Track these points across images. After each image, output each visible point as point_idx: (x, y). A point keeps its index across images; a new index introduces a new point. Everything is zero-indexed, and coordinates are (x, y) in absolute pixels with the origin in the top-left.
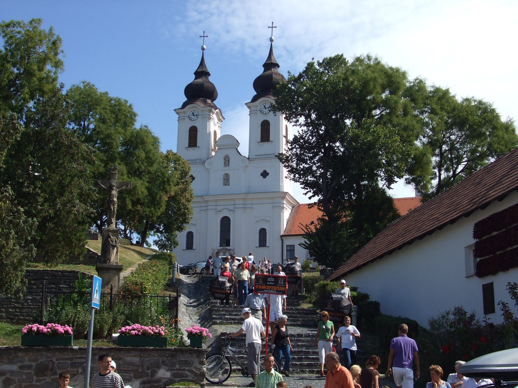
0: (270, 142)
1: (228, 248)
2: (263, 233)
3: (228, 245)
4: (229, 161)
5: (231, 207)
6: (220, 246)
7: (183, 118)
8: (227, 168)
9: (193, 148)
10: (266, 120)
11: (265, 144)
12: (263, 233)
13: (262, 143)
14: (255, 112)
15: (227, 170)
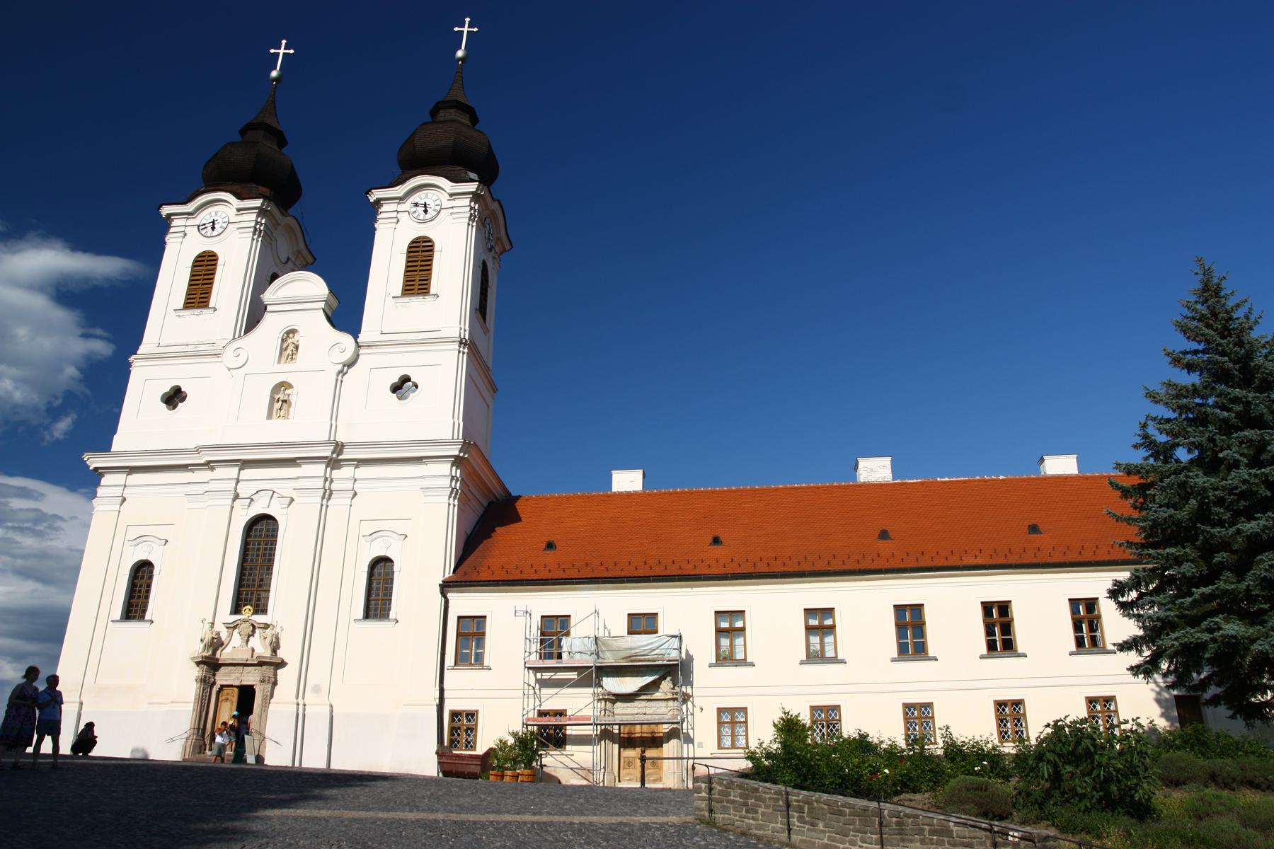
0: (429, 298)
1: (259, 619)
2: (380, 571)
3: (261, 609)
4: (297, 347)
5: (285, 489)
6: (236, 610)
7: (182, 229)
8: (287, 366)
9: (197, 311)
10: (424, 237)
11: (416, 302)
12: (380, 571)
13: (406, 299)
14: (394, 214)
15: (284, 372)
